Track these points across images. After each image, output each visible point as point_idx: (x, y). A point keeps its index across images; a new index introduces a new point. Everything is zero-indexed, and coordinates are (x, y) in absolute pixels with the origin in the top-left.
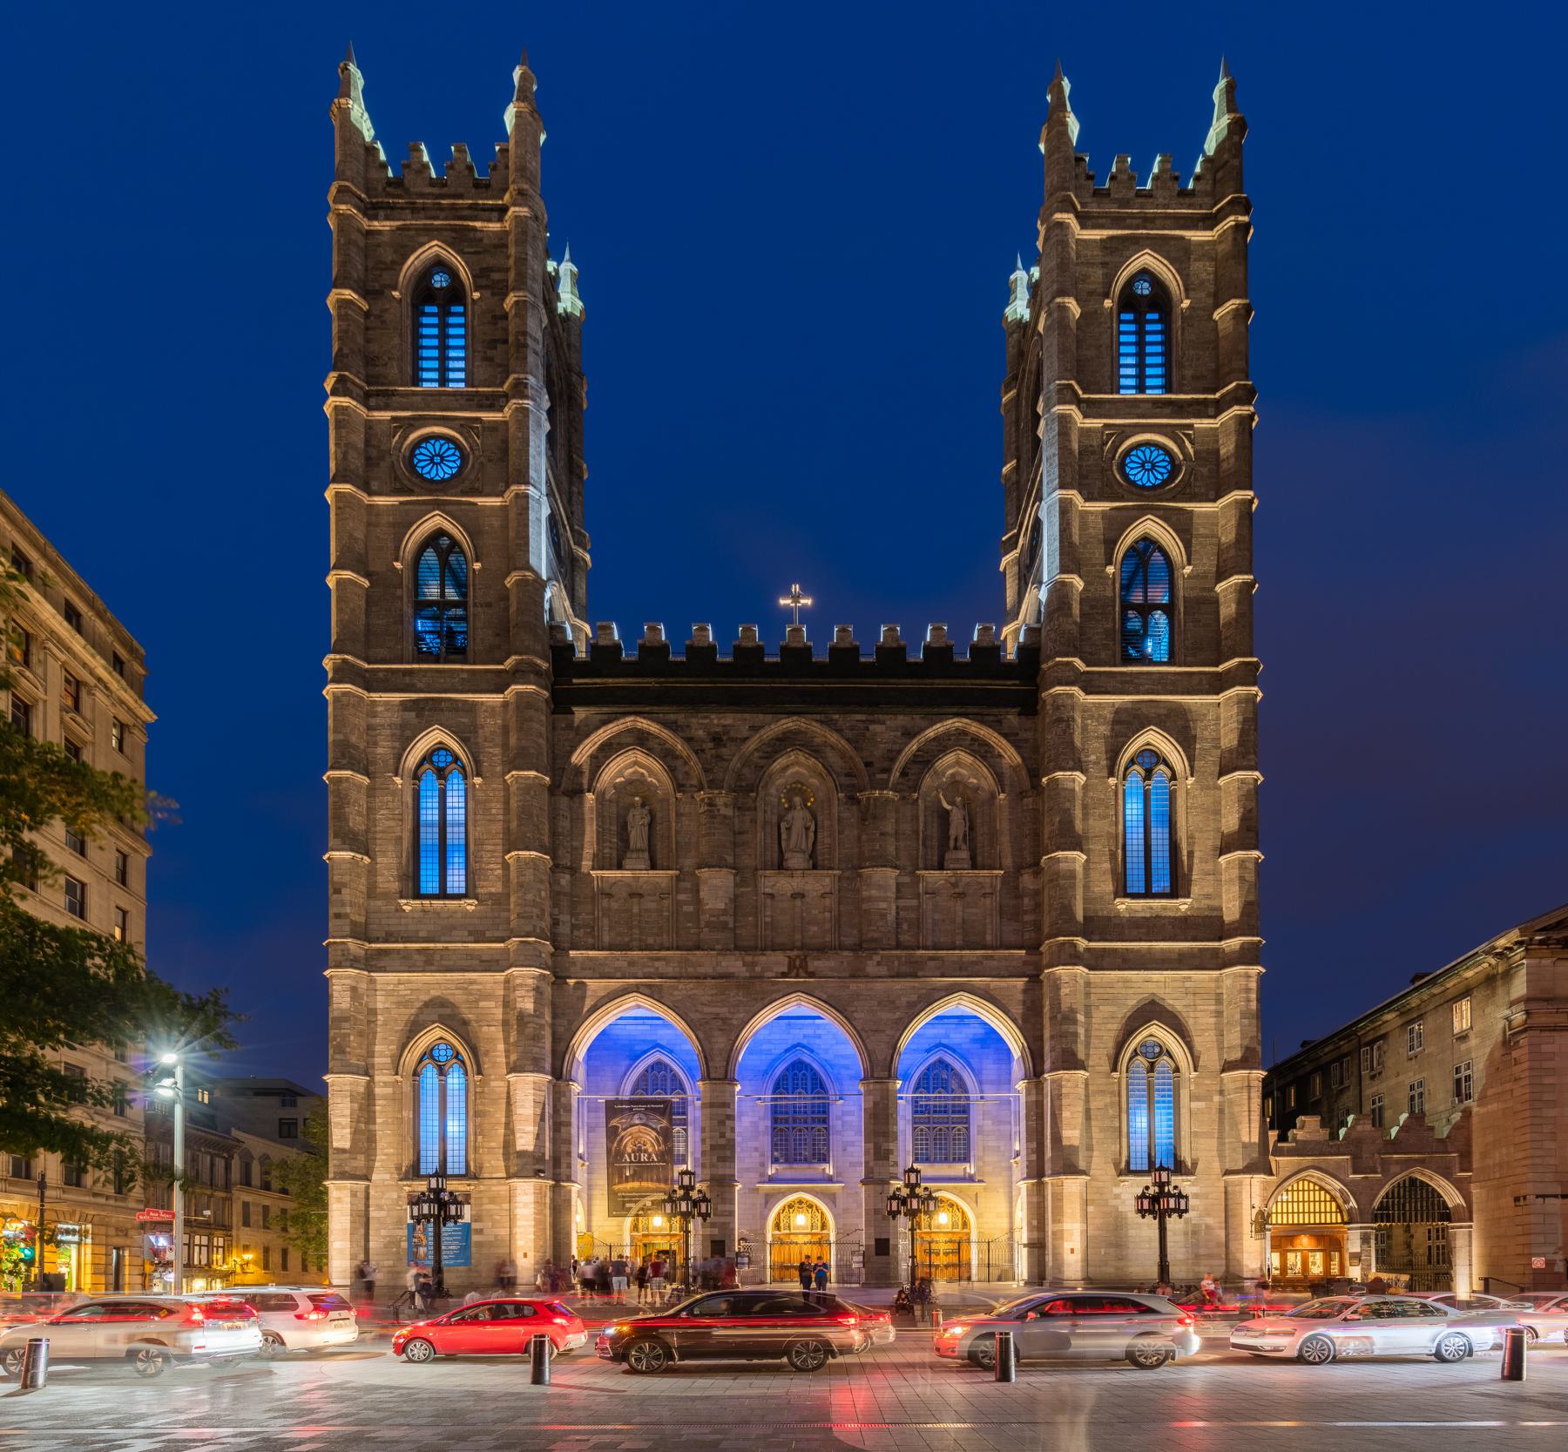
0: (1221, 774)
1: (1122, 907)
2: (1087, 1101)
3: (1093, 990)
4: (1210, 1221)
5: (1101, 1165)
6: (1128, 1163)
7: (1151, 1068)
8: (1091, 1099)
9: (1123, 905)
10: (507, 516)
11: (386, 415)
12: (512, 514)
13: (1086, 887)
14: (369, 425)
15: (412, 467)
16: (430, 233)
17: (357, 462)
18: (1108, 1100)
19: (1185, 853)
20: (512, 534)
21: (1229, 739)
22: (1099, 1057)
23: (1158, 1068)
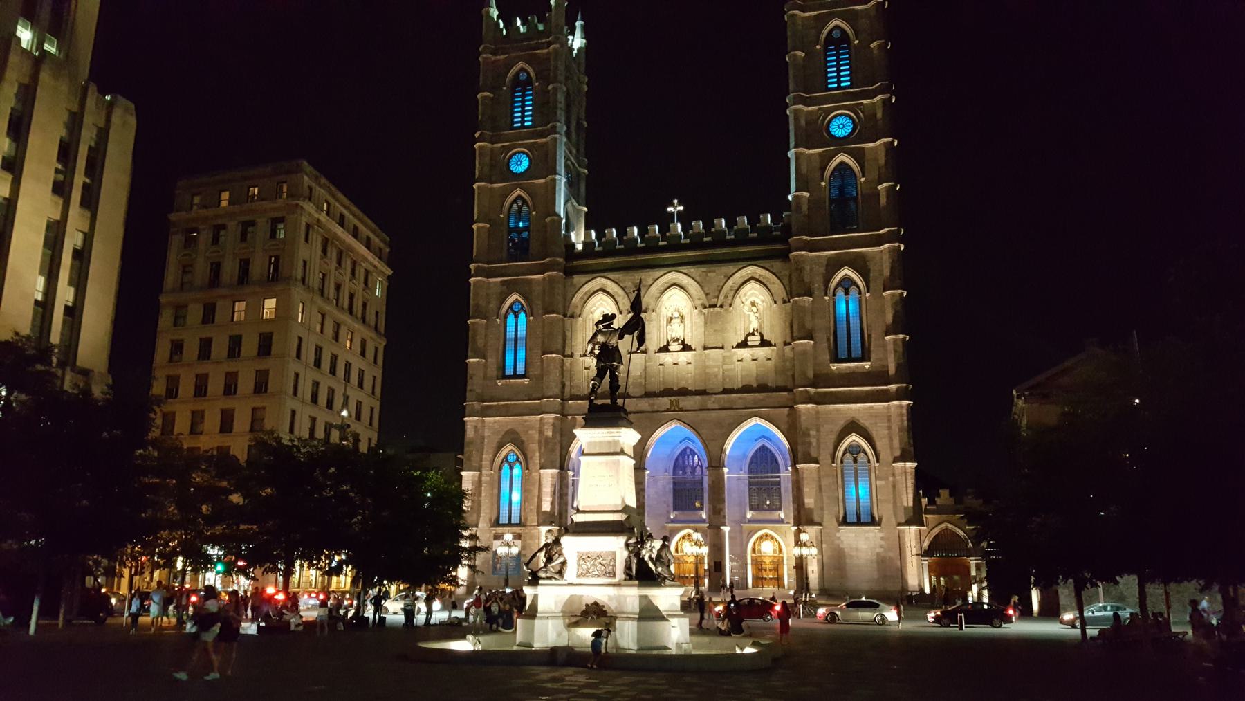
0: (885, 290)
2: (820, 480)
4: (891, 554)
5: (829, 520)
6: (845, 517)
7: (855, 460)
8: (822, 479)
9: (834, 367)
13: (815, 358)
14: (492, 150)
16: (520, 59)
17: (486, 169)
19: (866, 336)
21: (887, 272)
22: (825, 457)
23: (859, 460)
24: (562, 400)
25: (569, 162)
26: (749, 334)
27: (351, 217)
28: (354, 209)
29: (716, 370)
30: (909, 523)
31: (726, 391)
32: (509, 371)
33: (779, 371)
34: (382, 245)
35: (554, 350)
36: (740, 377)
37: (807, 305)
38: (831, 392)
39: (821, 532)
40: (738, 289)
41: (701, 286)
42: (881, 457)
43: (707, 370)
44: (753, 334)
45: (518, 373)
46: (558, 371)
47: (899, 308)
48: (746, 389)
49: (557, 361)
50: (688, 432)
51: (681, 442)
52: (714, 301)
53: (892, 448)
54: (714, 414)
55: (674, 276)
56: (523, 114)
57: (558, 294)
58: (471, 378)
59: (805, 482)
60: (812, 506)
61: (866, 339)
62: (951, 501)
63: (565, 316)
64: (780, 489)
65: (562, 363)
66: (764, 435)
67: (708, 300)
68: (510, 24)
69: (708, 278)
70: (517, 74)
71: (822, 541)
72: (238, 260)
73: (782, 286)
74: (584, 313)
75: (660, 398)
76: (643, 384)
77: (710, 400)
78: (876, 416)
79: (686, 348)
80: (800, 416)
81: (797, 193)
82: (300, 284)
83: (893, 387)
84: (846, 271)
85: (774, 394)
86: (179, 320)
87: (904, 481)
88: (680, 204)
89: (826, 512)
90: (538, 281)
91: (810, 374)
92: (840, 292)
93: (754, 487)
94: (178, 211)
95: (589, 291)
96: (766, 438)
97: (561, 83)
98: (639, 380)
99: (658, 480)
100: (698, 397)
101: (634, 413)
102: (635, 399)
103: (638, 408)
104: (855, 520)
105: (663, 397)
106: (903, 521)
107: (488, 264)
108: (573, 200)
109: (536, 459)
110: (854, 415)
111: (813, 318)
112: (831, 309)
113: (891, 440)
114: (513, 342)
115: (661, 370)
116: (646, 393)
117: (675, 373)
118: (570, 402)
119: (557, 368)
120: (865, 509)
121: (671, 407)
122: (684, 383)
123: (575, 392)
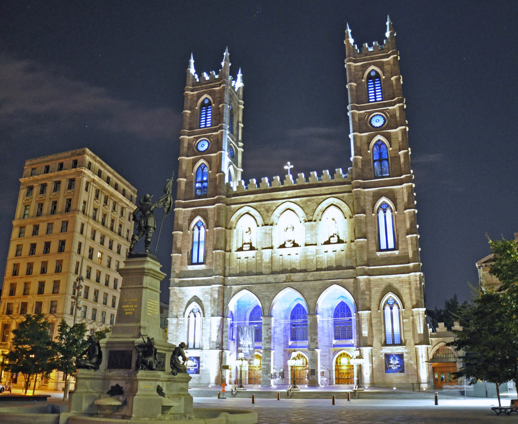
0: (405, 209)
1: (378, 255)
3: (371, 283)
4: (411, 362)
5: (376, 343)
6: (385, 341)
8: (373, 320)
9: (379, 254)
10: (217, 158)
11: (192, 137)
12: (219, 158)
15: (197, 148)
16: (204, 93)
18: (378, 320)
19: (396, 235)
20: (218, 163)
21: (406, 199)
22: (374, 306)
24: (225, 276)
25: (231, 144)
26: (331, 237)
27: (114, 178)
28: (116, 174)
29: (312, 257)
30: (420, 344)
31: (318, 270)
32: (195, 260)
33: (349, 257)
34: (132, 194)
35: (219, 247)
36: (326, 261)
37: (362, 219)
38: (377, 269)
39: (372, 351)
40: (324, 211)
41: (303, 210)
42: (406, 306)
43: (307, 258)
44: (333, 236)
45: (199, 262)
46: (221, 260)
47: (413, 219)
48: (329, 268)
49: (221, 254)
50: (298, 295)
51: (295, 301)
52: (310, 218)
53: (411, 300)
54: (311, 283)
55: (288, 205)
56: (206, 121)
57: (222, 216)
58: (174, 265)
59: (363, 321)
60: (367, 335)
61: (396, 237)
62: (445, 329)
63: (226, 228)
64: (352, 326)
65: (224, 256)
66: (343, 295)
67: (307, 218)
68: (200, 76)
69: (307, 205)
70: (204, 101)
71: (372, 355)
72: (51, 202)
73: (349, 209)
74: (237, 227)
75: (280, 275)
76: (271, 266)
77: (309, 275)
78: (402, 282)
79: (295, 245)
80: (360, 284)
81: (355, 157)
82: (81, 214)
83: (411, 265)
84: (384, 199)
85: (346, 271)
86: (21, 234)
87: (418, 319)
88: (291, 164)
89: (375, 339)
90: (211, 209)
91: (365, 259)
92: (381, 213)
93: (337, 326)
94: (25, 177)
95: (240, 214)
96: (343, 297)
97: (226, 103)
98: (268, 265)
99: (281, 324)
100: (301, 274)
101: (265, 283)
102: (265, 276)
103: (267, 281)
104: (391, 343)
105: (282, 273)
106: (417, 342)
107: (184, 200)
108: (234, 165)
109: (209, 310)
110: (390, 282)
111: (366, 226)
112: (376, 221)
113: (411, 295)
114: (197, 244)
115: (281, 258)
116: (272, 272)
117: (289, 260)
118: (229, 278)
119: (221, 258)
120: (397, 336)
121: (286, 280)
122: (294, 265)
123: (231, 272)
